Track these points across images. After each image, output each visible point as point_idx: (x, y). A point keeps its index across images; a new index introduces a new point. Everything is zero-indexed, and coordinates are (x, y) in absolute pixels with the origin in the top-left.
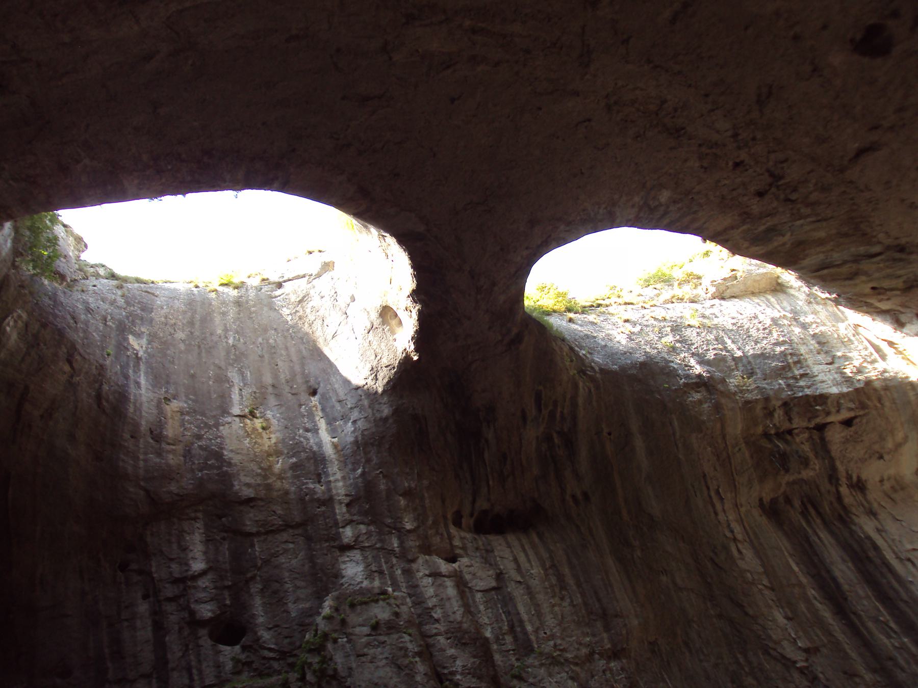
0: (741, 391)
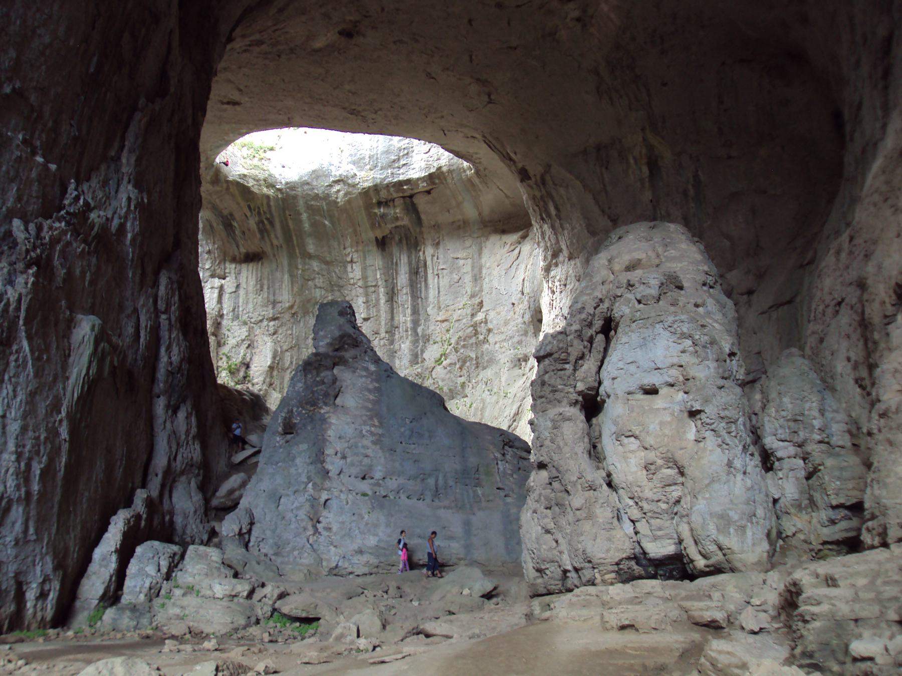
0: (363, 181)
